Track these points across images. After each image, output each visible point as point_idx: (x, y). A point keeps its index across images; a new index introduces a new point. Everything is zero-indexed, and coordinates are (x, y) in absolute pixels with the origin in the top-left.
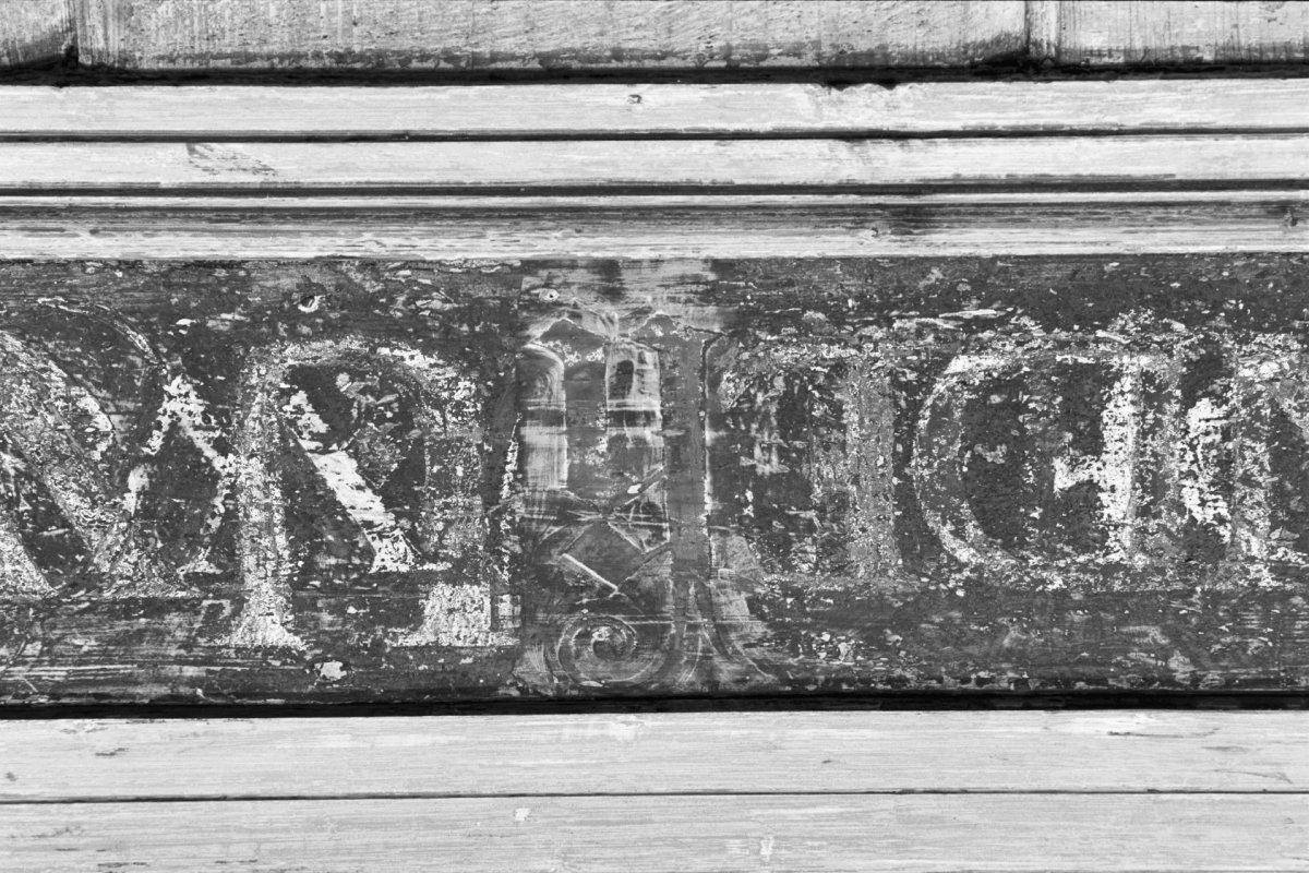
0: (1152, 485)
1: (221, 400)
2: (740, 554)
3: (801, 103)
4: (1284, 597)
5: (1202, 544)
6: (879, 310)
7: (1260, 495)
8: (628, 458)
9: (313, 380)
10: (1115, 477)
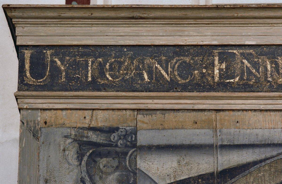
4: (278, 56)
7: (280, 67)
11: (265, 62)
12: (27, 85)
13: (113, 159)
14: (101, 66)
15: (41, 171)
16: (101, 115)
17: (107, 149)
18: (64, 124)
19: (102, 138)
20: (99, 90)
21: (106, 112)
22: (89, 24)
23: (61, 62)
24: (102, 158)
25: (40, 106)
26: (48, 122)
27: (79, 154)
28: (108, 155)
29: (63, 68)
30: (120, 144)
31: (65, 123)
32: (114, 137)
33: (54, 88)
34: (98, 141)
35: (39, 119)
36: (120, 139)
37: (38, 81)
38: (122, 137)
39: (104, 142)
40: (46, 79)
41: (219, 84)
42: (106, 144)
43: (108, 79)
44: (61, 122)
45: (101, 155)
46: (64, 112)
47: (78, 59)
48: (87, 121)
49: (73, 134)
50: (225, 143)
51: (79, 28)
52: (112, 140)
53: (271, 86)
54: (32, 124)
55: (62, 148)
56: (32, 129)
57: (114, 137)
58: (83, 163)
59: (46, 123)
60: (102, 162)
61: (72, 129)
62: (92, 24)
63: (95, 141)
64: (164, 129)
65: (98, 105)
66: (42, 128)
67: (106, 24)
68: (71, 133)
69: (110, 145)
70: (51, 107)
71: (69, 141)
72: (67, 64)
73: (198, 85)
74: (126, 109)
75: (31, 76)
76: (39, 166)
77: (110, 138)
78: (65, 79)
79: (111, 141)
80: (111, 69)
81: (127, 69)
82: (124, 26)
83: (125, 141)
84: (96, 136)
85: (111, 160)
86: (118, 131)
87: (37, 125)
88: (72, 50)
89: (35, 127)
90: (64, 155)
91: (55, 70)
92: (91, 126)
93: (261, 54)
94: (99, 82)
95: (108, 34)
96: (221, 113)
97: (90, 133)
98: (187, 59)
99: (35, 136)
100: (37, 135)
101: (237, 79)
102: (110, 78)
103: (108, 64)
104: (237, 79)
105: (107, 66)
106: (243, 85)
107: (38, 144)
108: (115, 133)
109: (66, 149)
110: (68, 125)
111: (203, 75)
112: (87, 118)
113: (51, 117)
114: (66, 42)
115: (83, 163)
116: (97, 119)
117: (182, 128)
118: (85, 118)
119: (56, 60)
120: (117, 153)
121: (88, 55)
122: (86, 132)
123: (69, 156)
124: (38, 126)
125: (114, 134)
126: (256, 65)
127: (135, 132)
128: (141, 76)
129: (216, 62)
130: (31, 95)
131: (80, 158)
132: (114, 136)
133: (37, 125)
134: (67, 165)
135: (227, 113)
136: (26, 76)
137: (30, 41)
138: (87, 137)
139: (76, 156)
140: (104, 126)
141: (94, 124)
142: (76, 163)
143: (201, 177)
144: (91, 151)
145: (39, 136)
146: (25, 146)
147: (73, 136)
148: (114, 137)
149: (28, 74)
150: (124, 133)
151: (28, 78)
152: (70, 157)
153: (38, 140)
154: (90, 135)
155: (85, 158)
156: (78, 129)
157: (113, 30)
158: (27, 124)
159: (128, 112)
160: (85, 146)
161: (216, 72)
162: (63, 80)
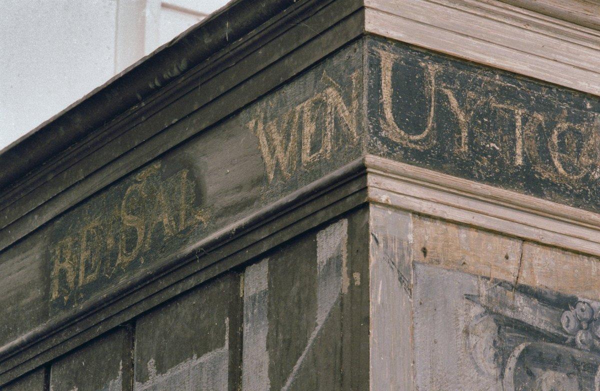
13: (568, 374)
15: (418, 375)
16: (540, 257)
17: (554, 349)
18: (464, 263)
19: (543, 318)
21: (548, 251)
22: (522, 21)
23: (458, 100)
24: (545, 369)
25: (417, 205)
26: (429, 250)
27: (499, 348)
28: (556, 363)
29: (461, 117)
30: (581, 341)
31: (466, 262)
32: (569, 320)
33: (444, 166)
34: (536, 324)
35: (410, 237)
36: (581, 328)
37: (411, 137)
38: (585, 325)
39: (548, 329)
40: (427, 136)
42: (553, 334)
43: (556, 170)
44: (458, 255)
46: (463, 234)
49: (484, 294)
51: (498, 25)
52: (564, 327)
54: (395, 247)
55: (462, 326)
56: (397, 260)
57: (569, 321)
58: (508, 373)
59: (424, 251)
60: (546, 379)
61: (482, 279)
62: (528, 23)
63: (530, 323)
65: (537, 231)
66: (418, 263)
67: (556, 31)
68: (479, 291)
69: (560, 340)
70: (439, 214)
71: (476, 310)
72: (470, 110)
74: (589, 255)
75: (395, 120)
76: (414, 363)
77: (559, 320)
78: (467, 147)
79: (561, 329)
80: (562, 145)
82: (591, 45)
83: (590, 336)
84: (531, 311)
85: (564, 378)
86: (575, 307)
87: (405, 253)
88: (480, 77)
89: (403, 256)
90: (466, 344)
92: (521, 282)
94: (540, 175)
95: (558, 57)
99: (404, 281)
100: (407, 279)
102: (561, 170)
103: (556, 132)
105: (555, 139)
107: (410, 302)
108: (568, 309)
109: (470, 329)
110: (472, 268)
112: (511, 258)
113: (435, 239)
114: (470, 52)
115: (508, 373)
116: (531, 265)
118: (507, 257)
119: (448, 92)
120: (574, 360)
122: (510, 294)
123: (478, 350)
124: (410, 257)
125: (567, 313)
130: (403, 172)
131: (501, 360)
132: (567, 317)
133: (405, 253)
134: (473, 373)
136: (384, 119)
137: (393, 29)
138: (513, 308)
139: (491, 352)
140: (546, 287)
142: (494, 372)
144: (522, 347)
145: (412, 283)
146: (382, 303)
147: (483, 298)
148: (569, 321)
149: (389, 115)
150: (587, 316)
151: (389, 126)
153: (411, 294)
154: (519, 305)
155: (512, 363)
156: (493, 282)
157: (567, 48)
158: (386, 246)
160: (509, 331)
162: (465, 148)
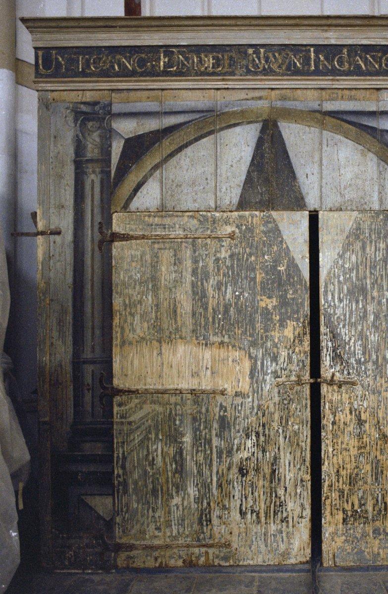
0: (209, 60)
1: (264, 67)
2: (234, 55)
3: (230, 87)
5: (206, 56)
6: (226, 73)
8: (240, 62)
9: (259, 68)
10: (211, 61)
11: (193, 57)
12: (40, 74)
14: (88, 61)
20: (86, 77)
28: (93, 120)
29: (63, 63)
32: (97, 108)
41: (163, 71)
45: (89, 120)
46: (66, 93)
47: (73, 56)
48: (80, 98)
50: (167, 110)
53: (196, 72)
64: (128, 102)
71: (69, 111)
73: (150, 73)
80: (94, 63)
81: (104, 62)
91: (59, 65)
93: (191, 51)
96: (166, 91)
97: (82, 106)
98: (143, 56)
101: (175, 68)
104: (175, 68)
106: (179, 72)
111: (153, 66)
117: (140, 102)
120: (99, 118)
121: (79, 54)
126: (187, 59)
127: (110, 104)
128: (113, 67)
129: (162, 57)
135: (169, 91)
141: (84, 100)
142: (73, 125)
143: (151, 132)
152: (69, 122)
155: (79, 122)
159: (106, 92)
161: (162, 63)
